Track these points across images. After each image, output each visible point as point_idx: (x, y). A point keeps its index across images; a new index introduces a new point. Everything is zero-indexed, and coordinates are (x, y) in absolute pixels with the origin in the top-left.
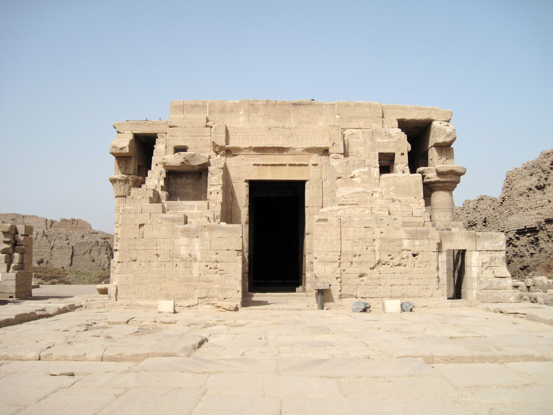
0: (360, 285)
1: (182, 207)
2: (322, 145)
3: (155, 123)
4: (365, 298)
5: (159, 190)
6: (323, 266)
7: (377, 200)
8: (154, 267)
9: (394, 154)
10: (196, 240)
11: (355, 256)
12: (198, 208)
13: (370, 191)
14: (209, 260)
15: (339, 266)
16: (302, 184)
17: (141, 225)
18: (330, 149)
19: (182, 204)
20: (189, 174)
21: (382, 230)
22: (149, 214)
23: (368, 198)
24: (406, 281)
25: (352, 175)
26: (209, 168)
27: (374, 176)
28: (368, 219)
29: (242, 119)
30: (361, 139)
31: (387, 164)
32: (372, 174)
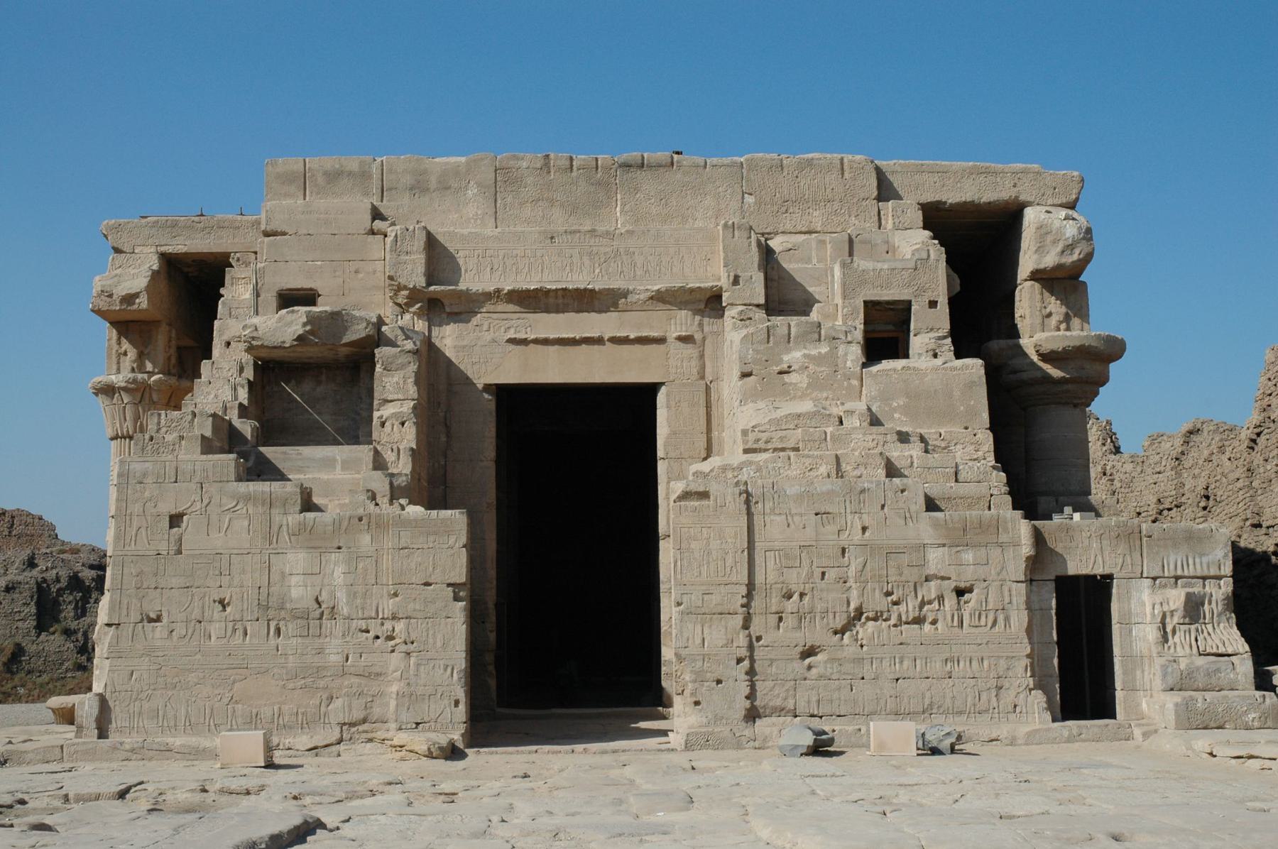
0: (805, 679)
1: (300, 463)
2: (703, 282)
3: (226, 224)
4: (821, 717)
5: (233, 416)
6: (699, 628)
7: (853, 436)
8: (213, 639)
9: (909, 303)
12: (346, 465)
13: (837, 411)
14: (373, 615)
15: (746, 626)
16: (650, 390)
17: (175, 520)
19: (301, 454)
20: (324, 371)
21: (867, 520)
22: (199, 485)
23: (829, 430)
24: (937, 667)
25: (785, 366)
26: (376, 351)
27: (845, 367)
28: (824, 489)
29: (471, 210)
30: (815, 261)
31: (889, 331)
32: (839, 363)
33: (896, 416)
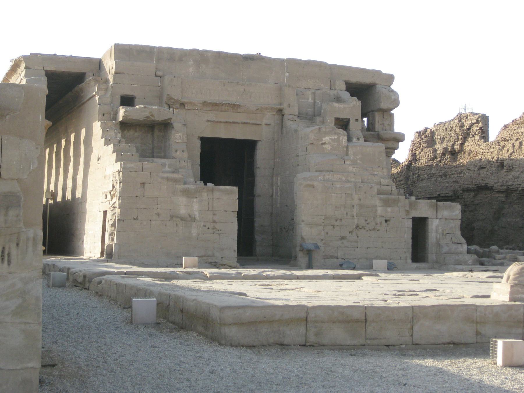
0: (340, 247)
10: (195, 200)
11: (336, 221)
15: (324, 230)
18: (284, 110)
20: (138, 127)
25: (323, 142)
33: (358, 161)
